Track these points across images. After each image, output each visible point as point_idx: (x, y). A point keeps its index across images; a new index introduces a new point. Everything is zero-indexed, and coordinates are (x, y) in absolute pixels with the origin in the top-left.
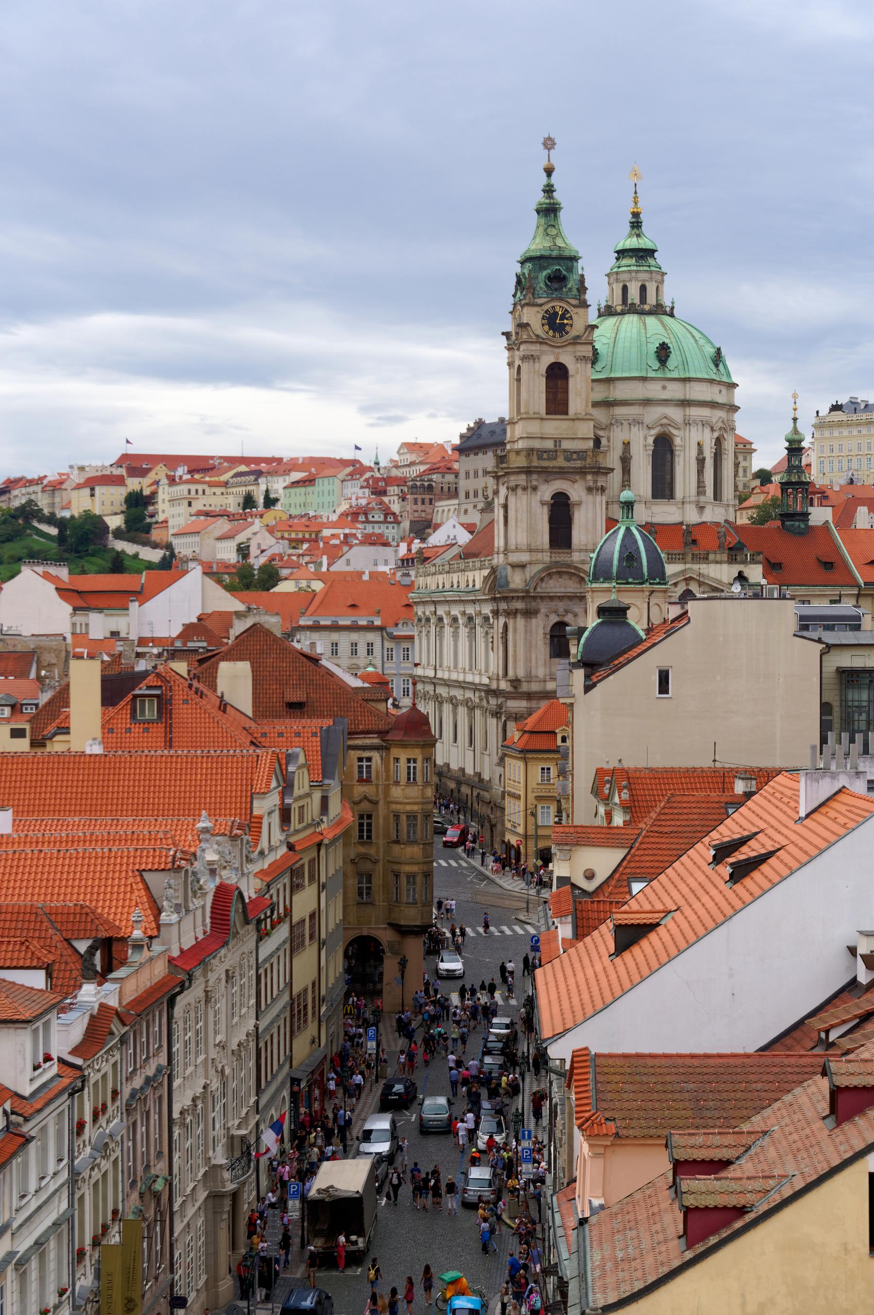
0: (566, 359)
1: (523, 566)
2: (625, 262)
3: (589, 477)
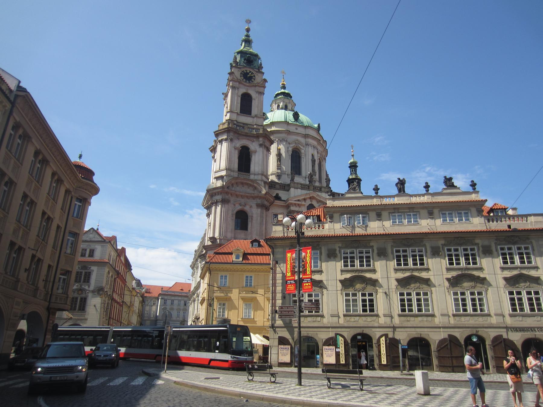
1: (221, 178)
3: (261, 139)
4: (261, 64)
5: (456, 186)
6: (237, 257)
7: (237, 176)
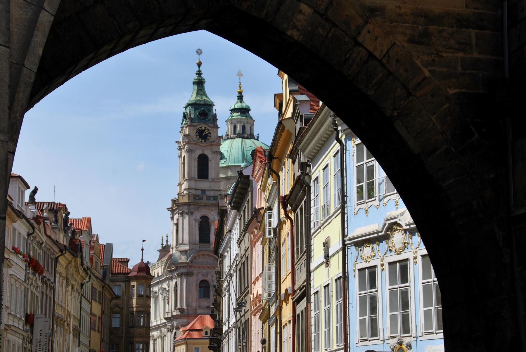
0: (208, 153)
2: (235, 114)
7: (198, 248)
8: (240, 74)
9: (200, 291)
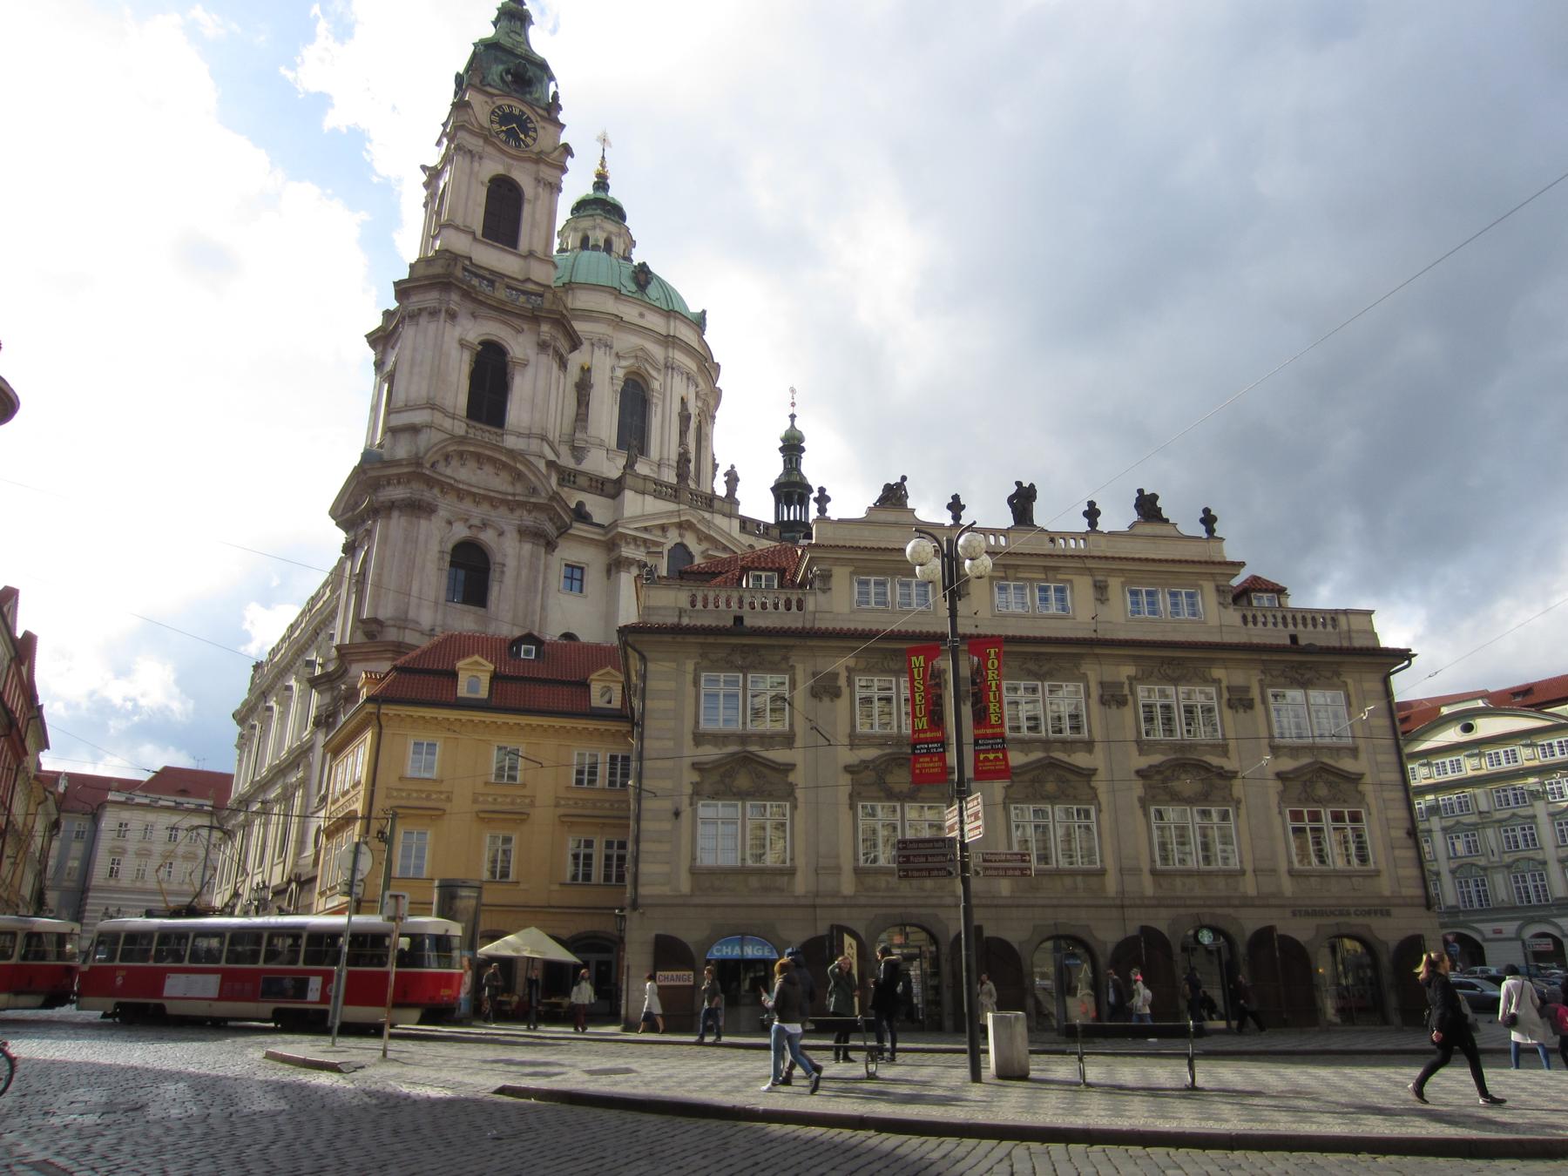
0: (523, 177)
1: (414, 429)
3: (545, 328)
4: (556, 95)
5: (1167, 521)
6: (473, 686)
7: (462, 433)
8: (604, 140)
9: (452, 580)
